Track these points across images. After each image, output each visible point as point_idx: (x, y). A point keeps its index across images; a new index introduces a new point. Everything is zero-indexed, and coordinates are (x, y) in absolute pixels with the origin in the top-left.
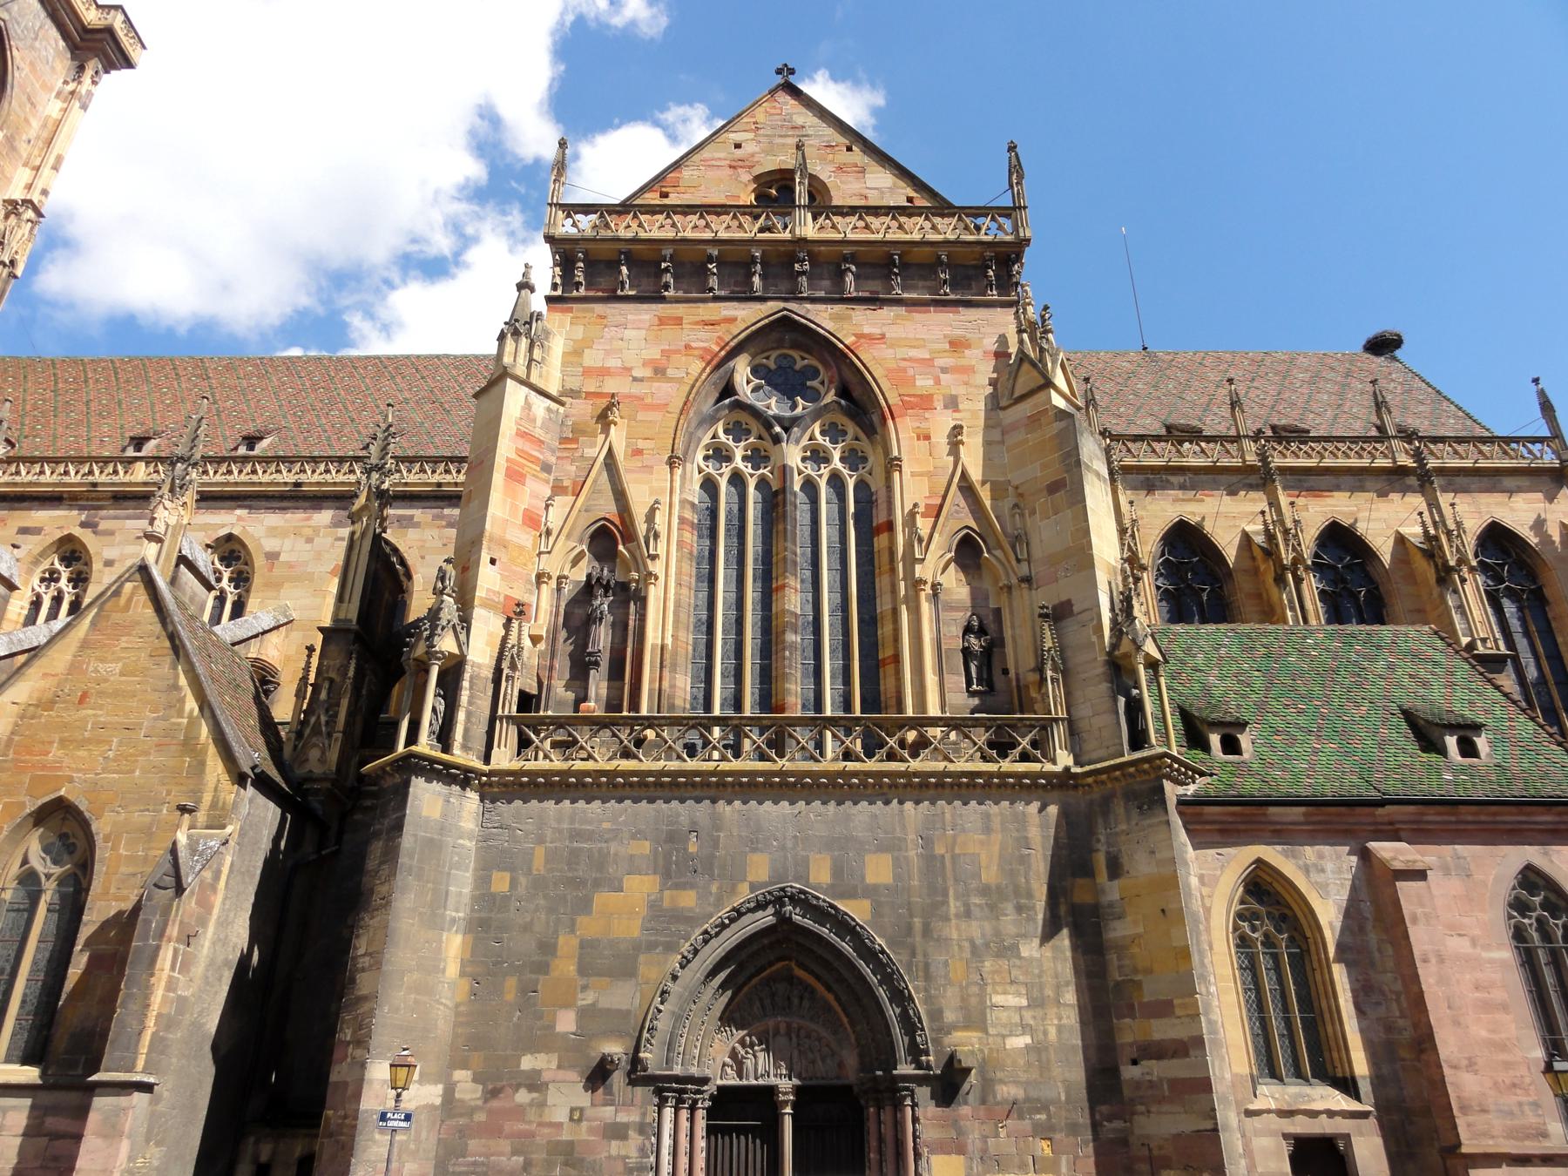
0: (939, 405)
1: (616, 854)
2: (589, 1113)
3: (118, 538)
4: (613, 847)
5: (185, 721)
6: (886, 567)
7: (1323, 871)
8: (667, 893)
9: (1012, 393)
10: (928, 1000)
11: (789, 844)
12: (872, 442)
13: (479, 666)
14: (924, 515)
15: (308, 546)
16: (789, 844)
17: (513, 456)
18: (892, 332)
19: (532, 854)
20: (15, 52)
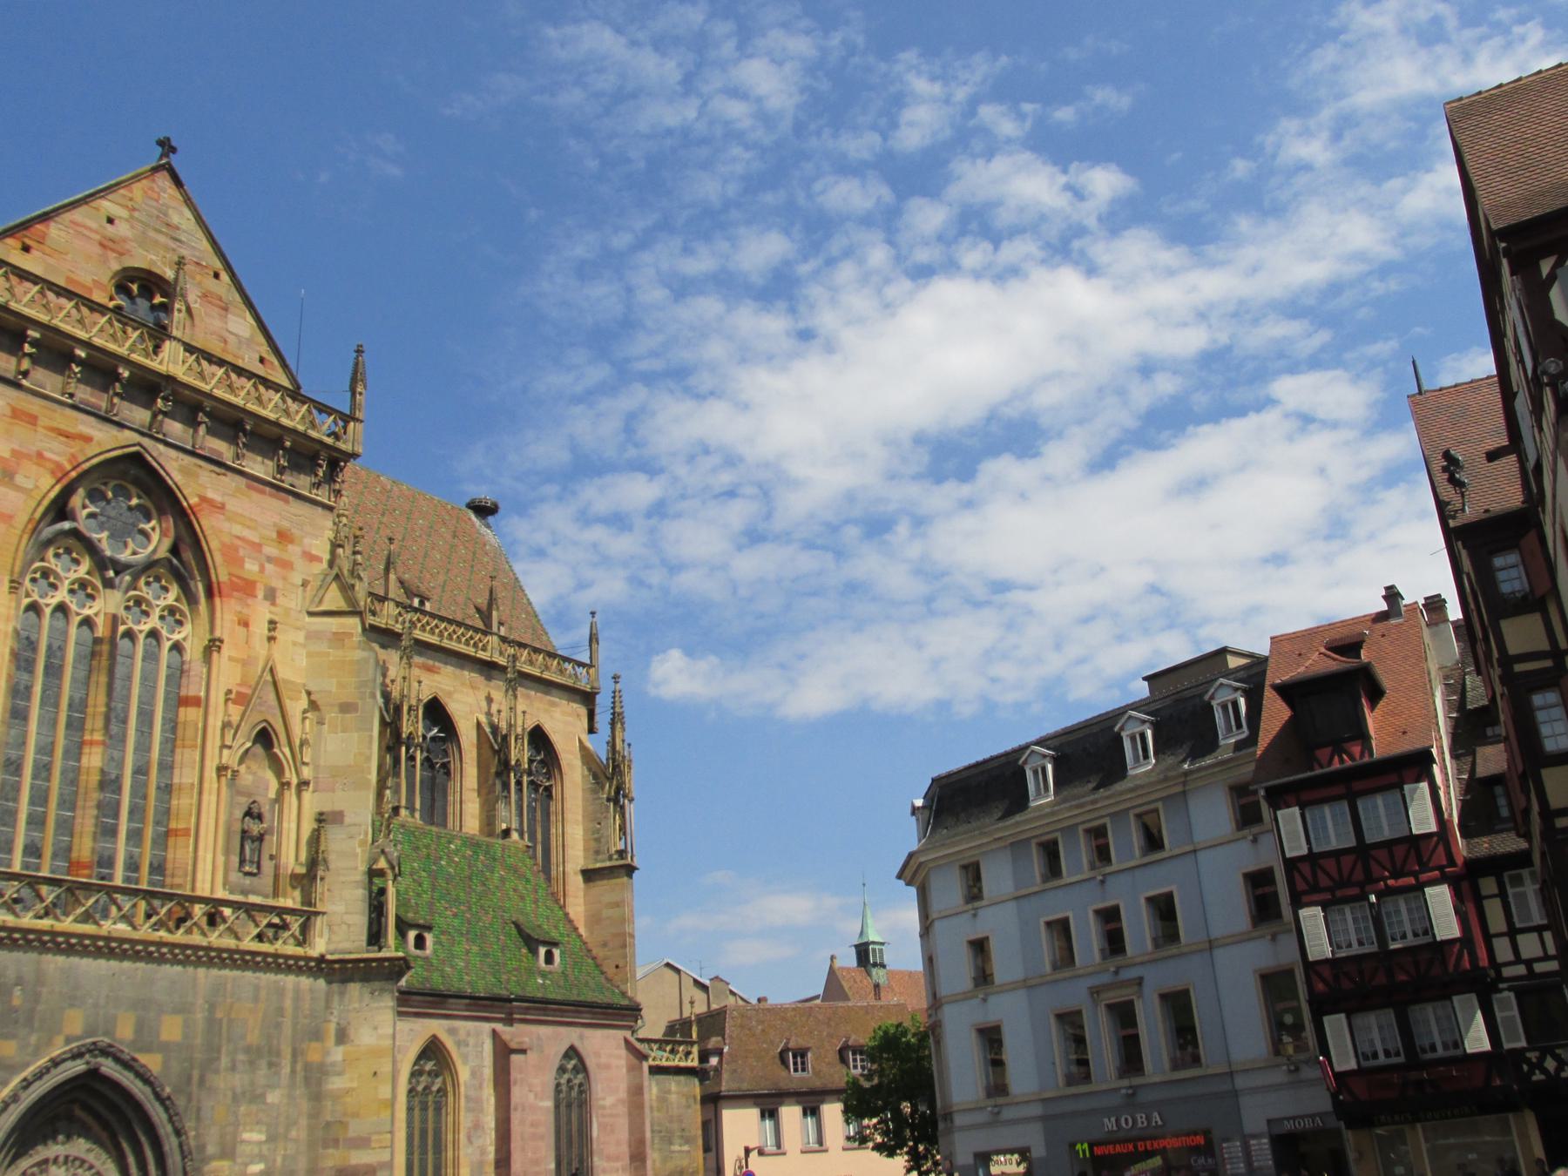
0: (260, 594)
7: (467, 1045)
9: (321, 601)
12: (192, 611)
14: (235, 702)
18: (232, 505)
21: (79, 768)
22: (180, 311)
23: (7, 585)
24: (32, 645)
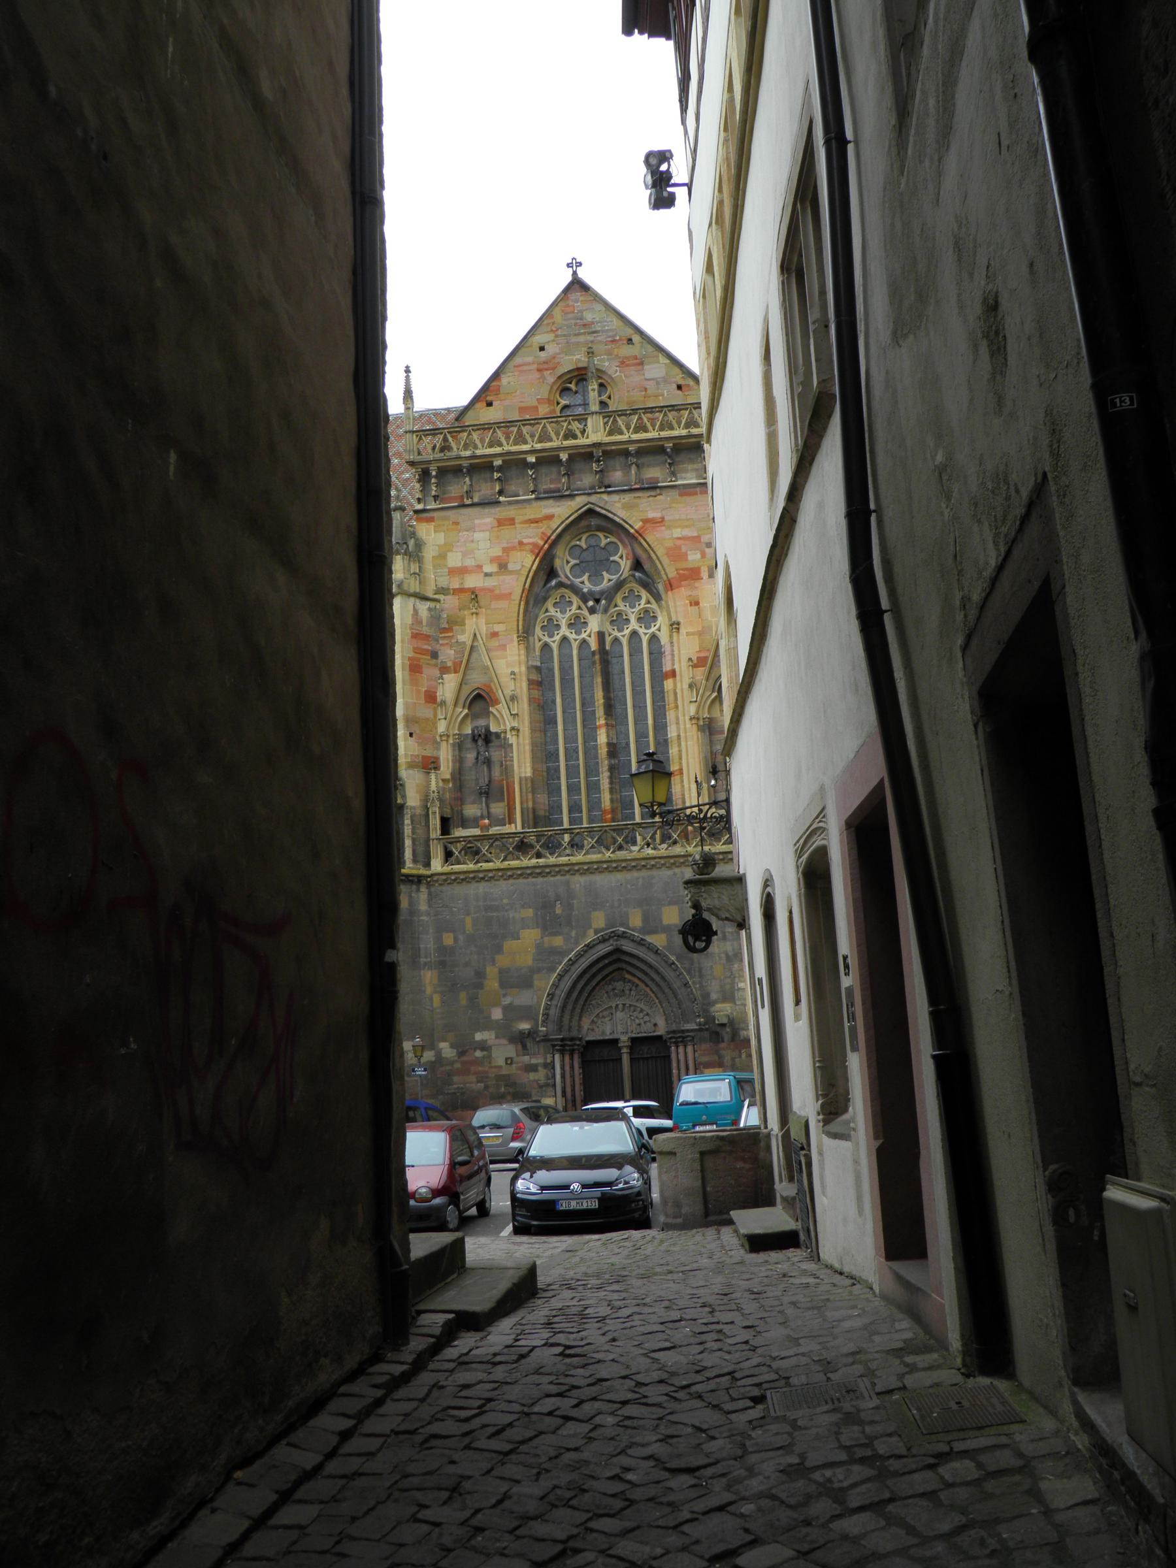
1: (513, 917)
2: (516, 1059)
6: (672, 705)
8: (546, 939)
10: (702, 987)
11: (616, 904)
12: (660, 606)
13: (414, 808)
14: (695, 666)
16: (616, 904)
21: (597, 745)
22: (593, 390)
23: (516, 639)
24: (552, 670)
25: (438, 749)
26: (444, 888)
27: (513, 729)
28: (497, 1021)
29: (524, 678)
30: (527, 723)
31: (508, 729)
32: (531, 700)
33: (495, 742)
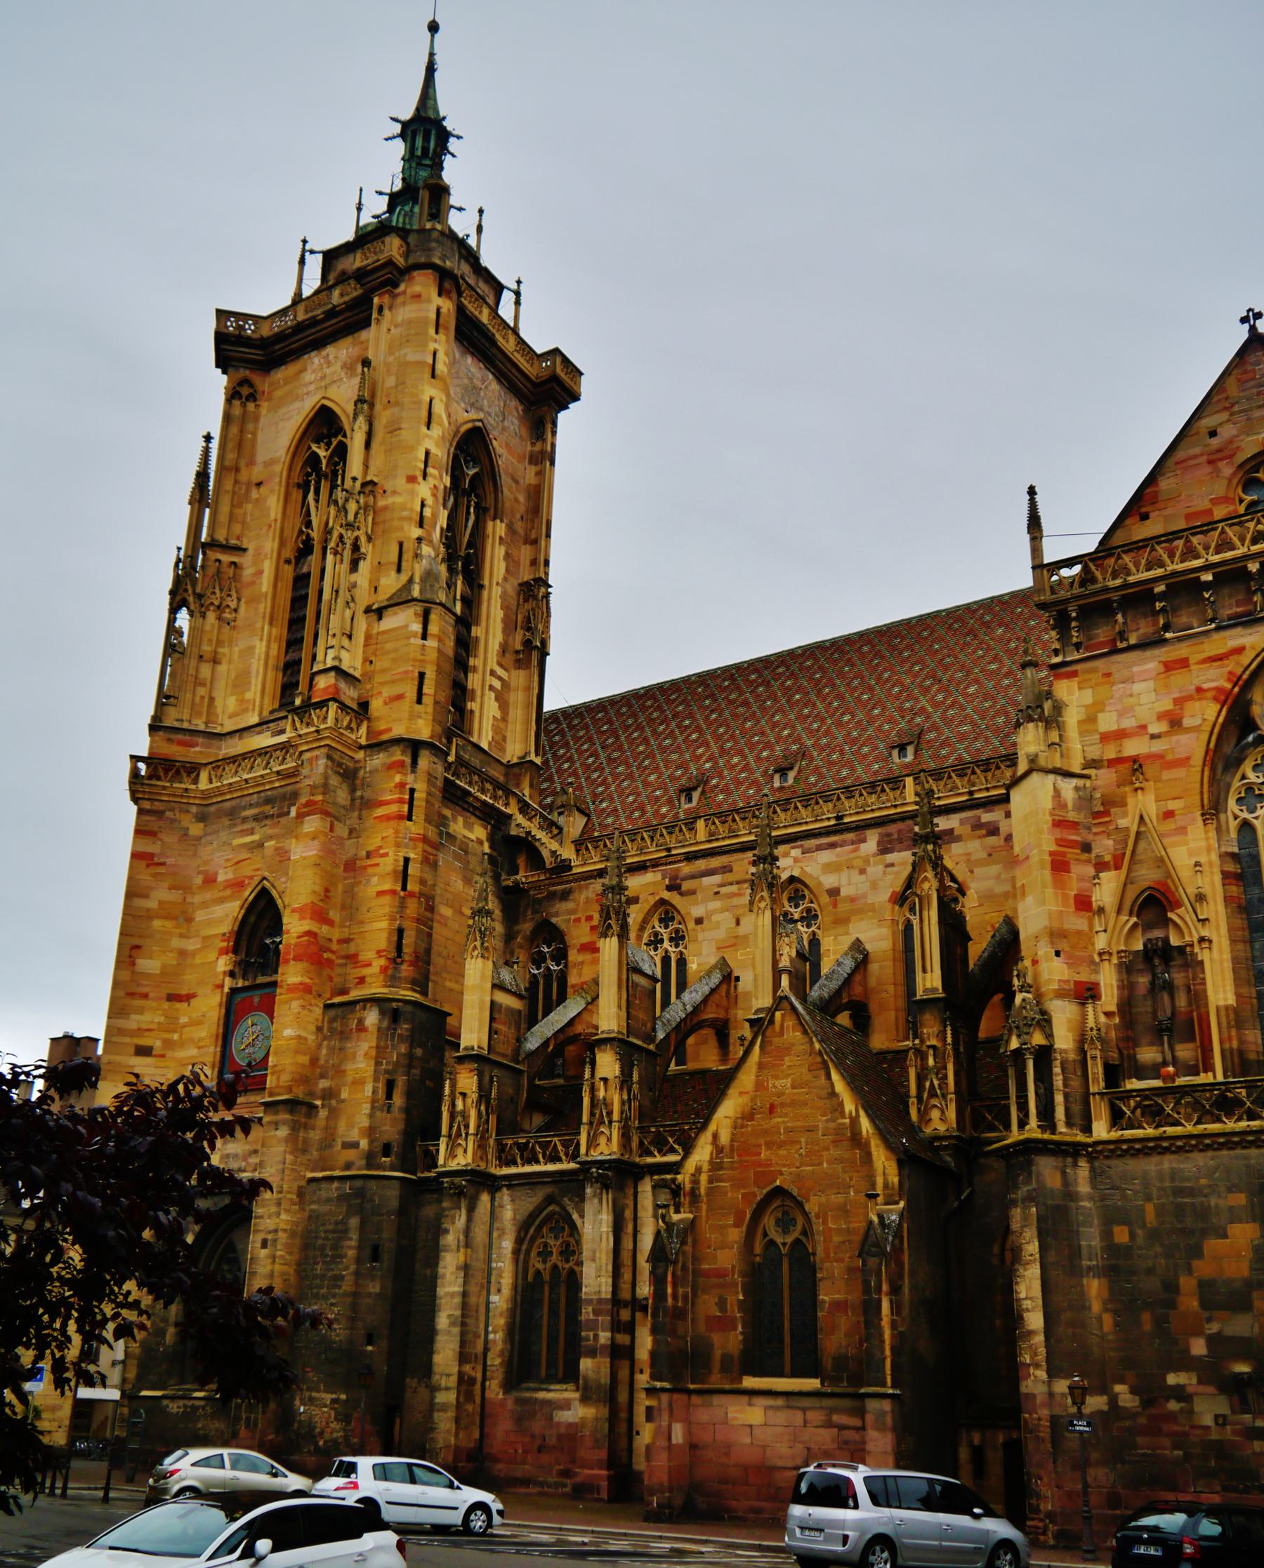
1: (1217, 1205)
2: (1231, 1418)
3: (699, 896)
4: (1213, 1201)
5: (847, 1121)
13: (1065, 1051)
15: (863, 878)
17: (1054, 848)
19: (1143, 1210)
20: (495, 443)
25: (1097, 972)
26: (1113, 1162)
27: (1202, 940)
28: (1199, 1358)
29: (1217, 870)
30: (1224, 930)
31: (1195, 940)
32: (1228, 900)
33: (1178, 961)
